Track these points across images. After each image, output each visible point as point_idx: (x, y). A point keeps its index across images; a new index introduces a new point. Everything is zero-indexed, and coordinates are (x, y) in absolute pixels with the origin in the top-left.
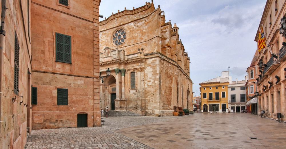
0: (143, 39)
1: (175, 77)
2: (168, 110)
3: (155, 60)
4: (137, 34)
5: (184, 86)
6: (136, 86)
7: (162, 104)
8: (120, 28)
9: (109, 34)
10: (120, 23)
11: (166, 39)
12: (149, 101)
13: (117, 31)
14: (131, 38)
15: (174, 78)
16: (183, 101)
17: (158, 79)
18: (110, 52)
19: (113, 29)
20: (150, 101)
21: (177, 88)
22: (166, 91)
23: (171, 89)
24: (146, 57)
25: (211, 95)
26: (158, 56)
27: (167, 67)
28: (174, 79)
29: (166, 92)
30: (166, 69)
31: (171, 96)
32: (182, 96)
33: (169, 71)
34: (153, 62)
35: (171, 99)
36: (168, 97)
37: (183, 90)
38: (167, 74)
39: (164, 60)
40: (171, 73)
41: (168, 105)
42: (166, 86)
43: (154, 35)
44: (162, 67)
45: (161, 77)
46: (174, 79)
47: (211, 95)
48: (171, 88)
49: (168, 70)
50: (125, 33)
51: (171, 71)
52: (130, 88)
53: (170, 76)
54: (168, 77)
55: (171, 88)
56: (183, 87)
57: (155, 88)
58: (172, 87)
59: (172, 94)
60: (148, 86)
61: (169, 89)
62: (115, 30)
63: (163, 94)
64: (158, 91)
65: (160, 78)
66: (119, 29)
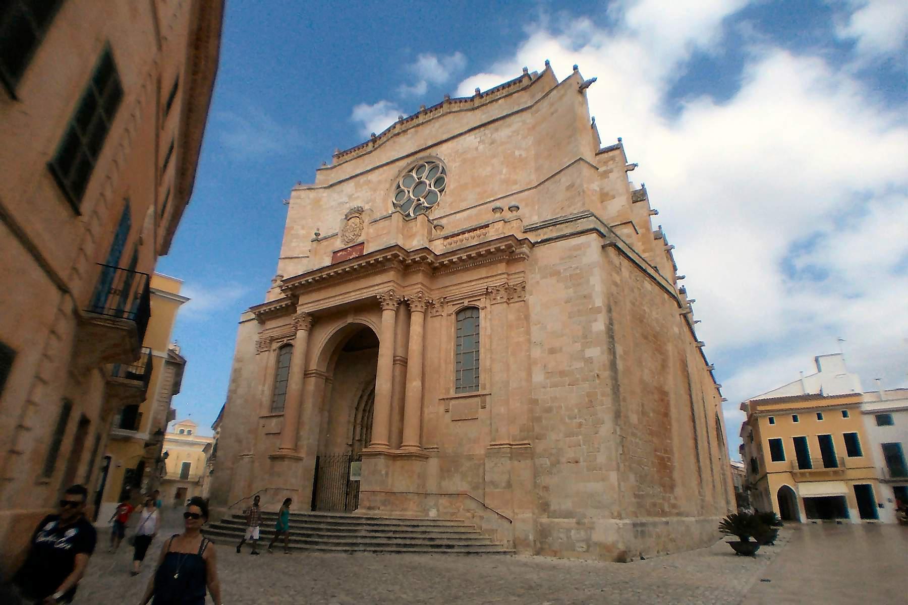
0: (515, 182)
2: (664, 519)
3: (578, 247)
4: (489, 169)
6: (482, 377)
7: (632, 477)
8: (421, 159)
9: (380, 182)
11: (614, 197)
12: (558, 462)
13: (411, 171)
15: (670, 347)
17: (604, 338)
18: (365, 224)
19: (397, 163)
20: (564, 460)
24: (533, 237)
25: (800, 443)
26: (592, 226)
27: (636, 290)
29: (644, 413)
31: (671, 439)
34: (570, 257)
35: (668, 450)
36: (655, 440)
38: (641, 321)
42: (642, 381)
43: (566, 160)
44: (616, 284)
47: (800, 443)
50: (443, 171)
51: (654, 313)
52: (447, 390)
53: (655, 336)
57: (586, 385)
59: (670, 424)
60: (549, 374)
62: (404, 168)
63: (634, 418)
64: (608, 402)
65: (610, 333)
66: (421, 163)
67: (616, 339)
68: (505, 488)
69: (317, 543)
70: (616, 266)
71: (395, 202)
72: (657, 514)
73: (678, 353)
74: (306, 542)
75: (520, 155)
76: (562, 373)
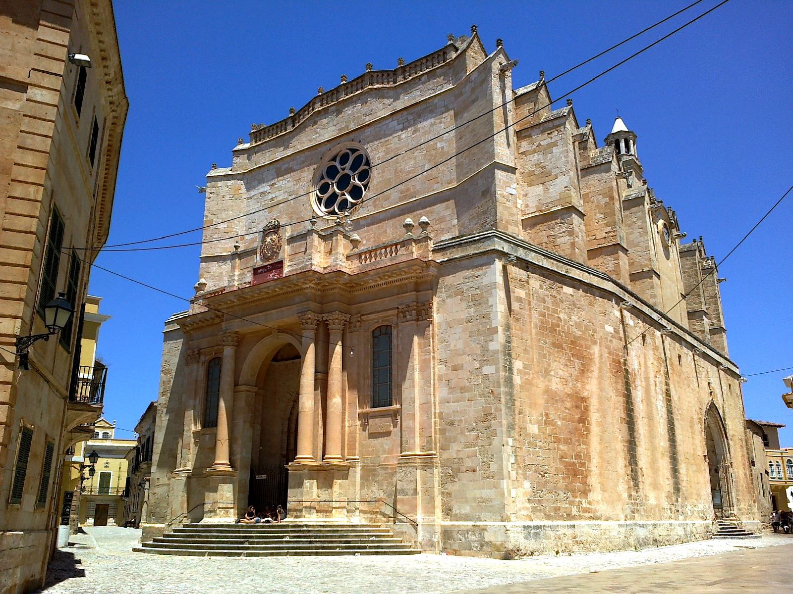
1: (608, 347)
5: (673, 393)
7: (527, 485)
10: (348, 122)
14: (389, 179)
15: (596, 350)
16: (675, 471)
20: (463, 469)
21: (621, 399)
22: (547, 415)
23: (586, 409)
28: (597, 355)
30: (548, 309)
32: (663, 443)
33: (562, 316)
37: (670, 411)
39: (526, 265)
40: (578, 325)
41: (567, 489)
42: (547, 391)
45: (515, 343)
46: (597, 355)
48: (583, 399)
49: (555, 311)
50: (368, 163)
51: (575, 318)
53: (572, 343)
54: (554, 345)
55: (580, 403)
56: (668, 394)
58: (585, 394)
59: (588, 430)
61: (568, 405)
63: (533, 429)
67: (513, 355)
68: (412, 495)
69: (248, 548)
70: (521, 281)
71: (319, 195)
72: (562, 518)
73: (609, 353)
74: (238, 548)
75: (443, 148)
76: (463, 389)
